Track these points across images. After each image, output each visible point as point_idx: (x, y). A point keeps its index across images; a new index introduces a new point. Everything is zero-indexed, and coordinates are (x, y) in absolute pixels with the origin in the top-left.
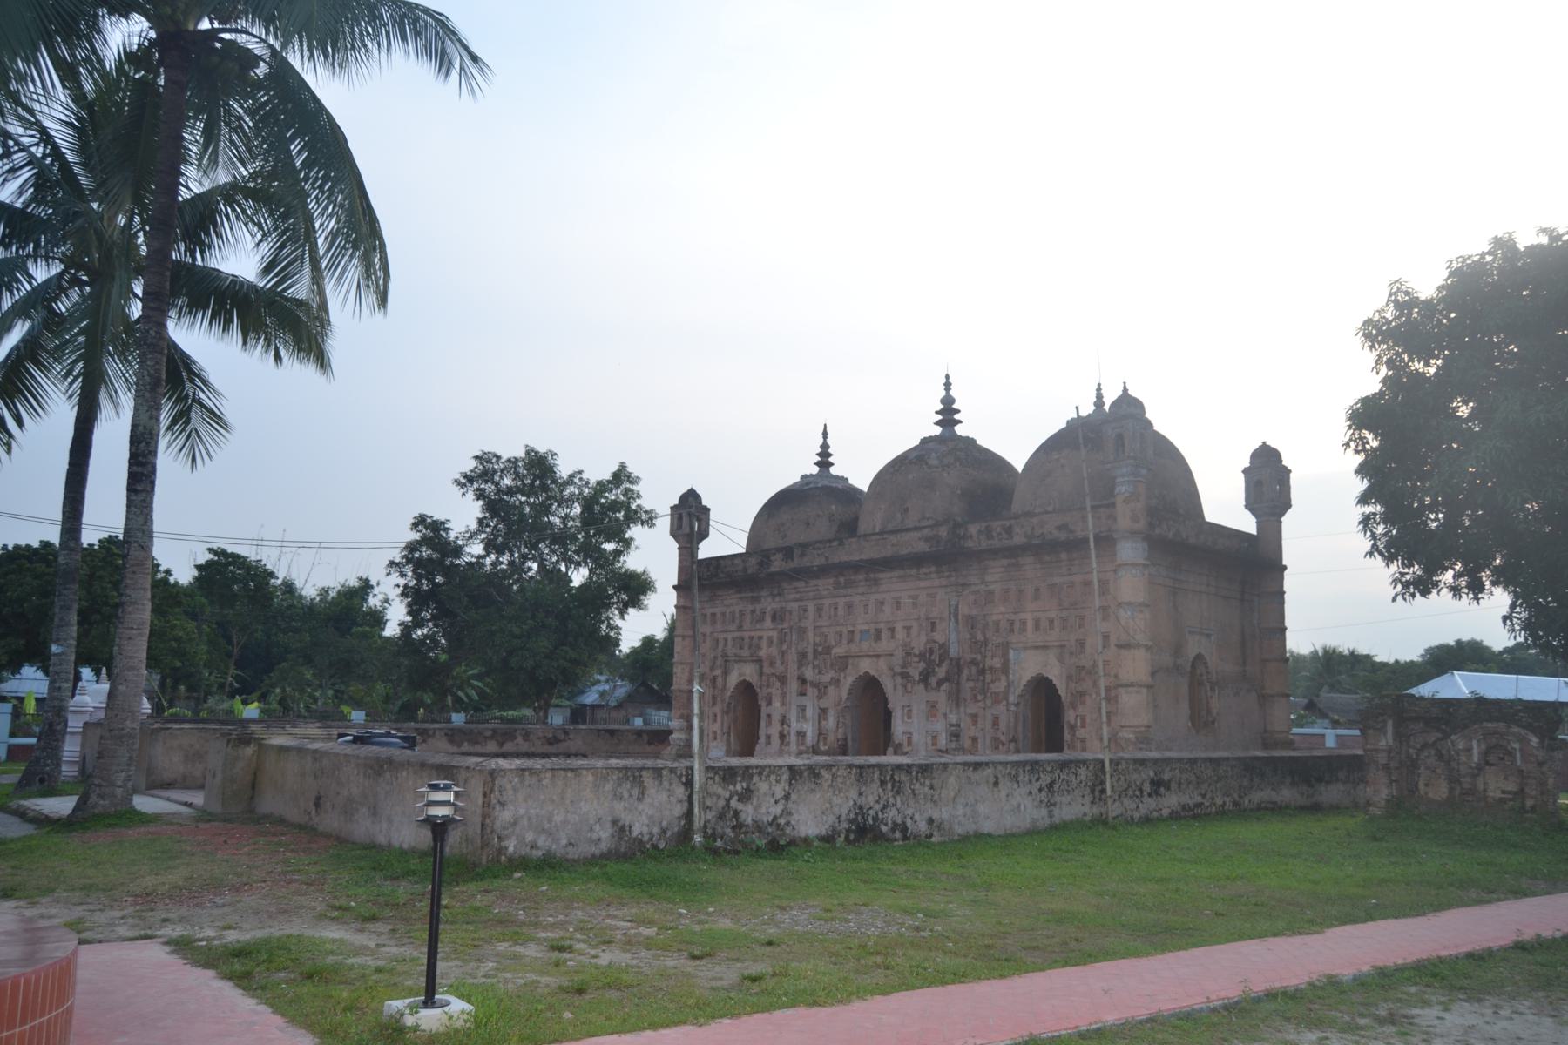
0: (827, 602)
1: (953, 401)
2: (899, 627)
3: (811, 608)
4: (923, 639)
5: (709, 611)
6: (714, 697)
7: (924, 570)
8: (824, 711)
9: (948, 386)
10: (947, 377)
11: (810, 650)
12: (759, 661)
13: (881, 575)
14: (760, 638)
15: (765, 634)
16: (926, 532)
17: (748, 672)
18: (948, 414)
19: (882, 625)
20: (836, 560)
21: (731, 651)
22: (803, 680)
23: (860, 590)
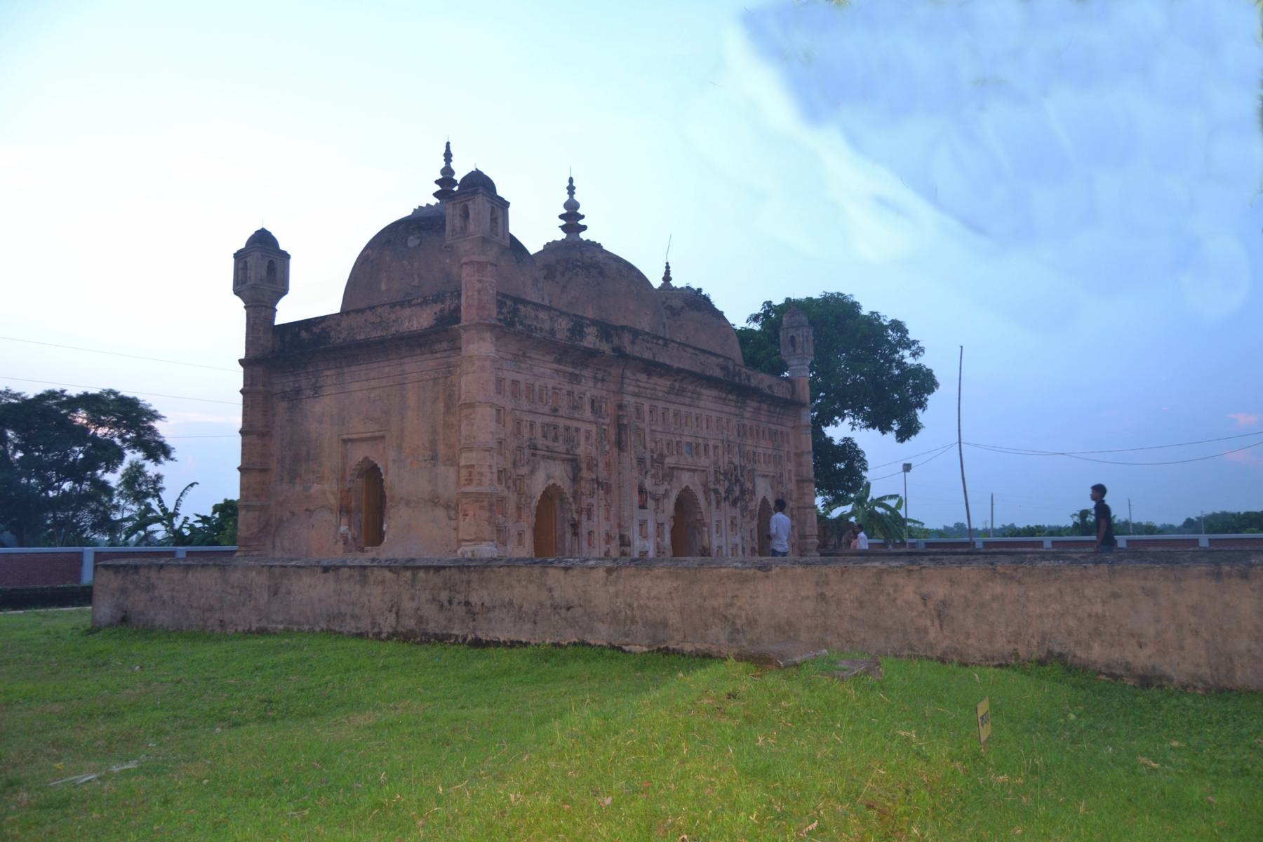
0: (660, 405)
1: (577, 205)
2: (711, 443)
3: (646, 408)
4: (726, 458)
5: (510, 376)
6: (519, 508)
7: (730, 397)
8: (660, 525)
9: (571, 189)
10: (571, 180)
11: (648, 455)
12: (574, 463)
13: (705, 392)
14: (577, 430)
15: (584, 427)
16: (721, 360)
17: (558, 473)
18: (572, 218)
19: (700, 441)
20: (661, 360)
21: (541, 442)
22: (642, 491)
23: (687, 401)
